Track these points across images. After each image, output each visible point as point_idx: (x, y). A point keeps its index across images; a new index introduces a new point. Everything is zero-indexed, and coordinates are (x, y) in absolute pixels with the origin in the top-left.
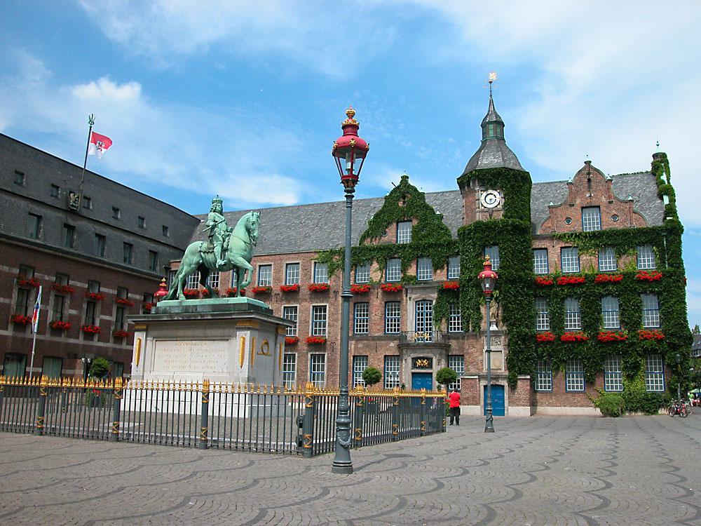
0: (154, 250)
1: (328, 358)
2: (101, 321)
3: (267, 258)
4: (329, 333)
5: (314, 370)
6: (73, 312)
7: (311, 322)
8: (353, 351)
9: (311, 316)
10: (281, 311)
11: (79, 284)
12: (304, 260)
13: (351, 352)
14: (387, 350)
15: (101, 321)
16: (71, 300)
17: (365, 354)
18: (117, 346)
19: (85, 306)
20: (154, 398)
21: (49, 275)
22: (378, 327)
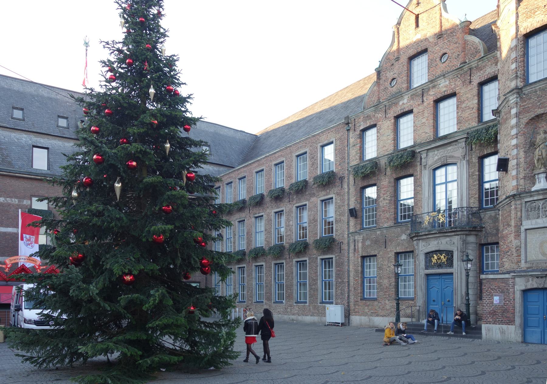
1: (336, 263)
3: (279, 154)
4: (337, 231)
5: (325, 278)
8: (360, 250)
10: (292, 212)
12: (311, 146)
13: (358, 252)
17: (373, 253)
22: (388, 215)
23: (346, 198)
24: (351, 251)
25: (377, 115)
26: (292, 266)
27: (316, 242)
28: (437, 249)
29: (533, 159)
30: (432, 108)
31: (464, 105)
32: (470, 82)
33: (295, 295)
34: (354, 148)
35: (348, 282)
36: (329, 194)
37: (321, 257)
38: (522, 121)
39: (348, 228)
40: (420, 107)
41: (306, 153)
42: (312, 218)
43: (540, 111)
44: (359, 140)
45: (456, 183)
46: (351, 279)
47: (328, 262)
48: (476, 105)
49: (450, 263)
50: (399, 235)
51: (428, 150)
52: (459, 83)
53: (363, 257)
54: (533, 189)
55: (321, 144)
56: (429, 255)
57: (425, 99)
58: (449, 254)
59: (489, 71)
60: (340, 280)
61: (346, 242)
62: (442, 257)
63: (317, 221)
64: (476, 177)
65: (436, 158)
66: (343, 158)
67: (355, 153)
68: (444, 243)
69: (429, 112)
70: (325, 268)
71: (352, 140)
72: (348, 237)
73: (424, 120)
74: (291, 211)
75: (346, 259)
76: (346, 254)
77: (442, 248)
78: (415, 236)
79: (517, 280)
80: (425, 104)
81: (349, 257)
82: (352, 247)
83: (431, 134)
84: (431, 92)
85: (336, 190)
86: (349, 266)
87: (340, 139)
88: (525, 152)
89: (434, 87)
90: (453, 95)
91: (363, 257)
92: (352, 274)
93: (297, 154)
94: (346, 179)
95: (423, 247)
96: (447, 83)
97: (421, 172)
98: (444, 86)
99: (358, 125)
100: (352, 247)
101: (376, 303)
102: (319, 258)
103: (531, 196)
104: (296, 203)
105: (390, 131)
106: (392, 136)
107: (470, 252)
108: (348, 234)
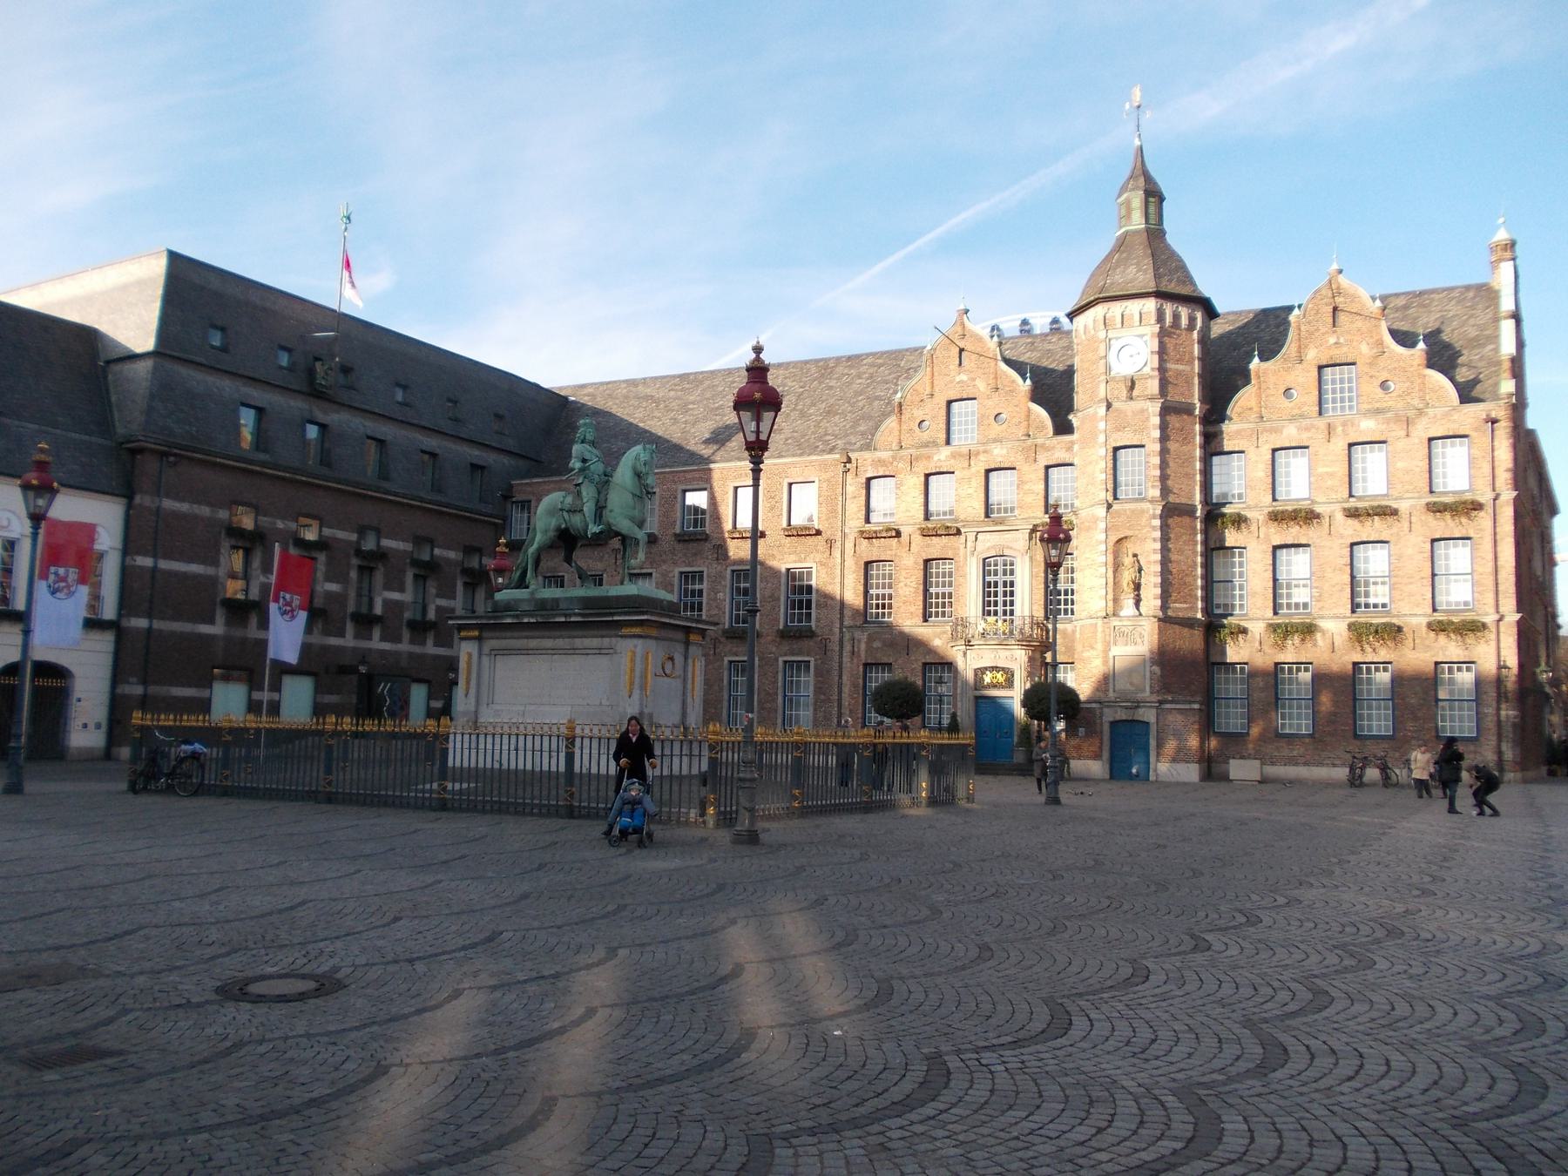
0: (481, 463)
2: (386, 603)
4: (818, 620)
6: (333, 587)
7: (783, 599)
8: (863, 654)
9: (783, 588)
10: (724, 578)
11: (341, 534)
15: (386, 603)
16: (329, 564)
17: (885, 660)
18: (417, 649)
19: (353, 574)
20: (497, 747)
21: (283, 518)
22: (913, 609)
26: (721, 667)
35: (840, 700)
36: (805, 560)
42: (767, 593)
61: (836, 638)
63: (778, 599)
74: (721, 576)
76: (836, 658)
81: (841, 664)
85: (818, 557)
86: (840, 677)
91: (866, 665)
92: (846, 690)
94: (838, 544)
100: (847, 648)
102: (781, 659)
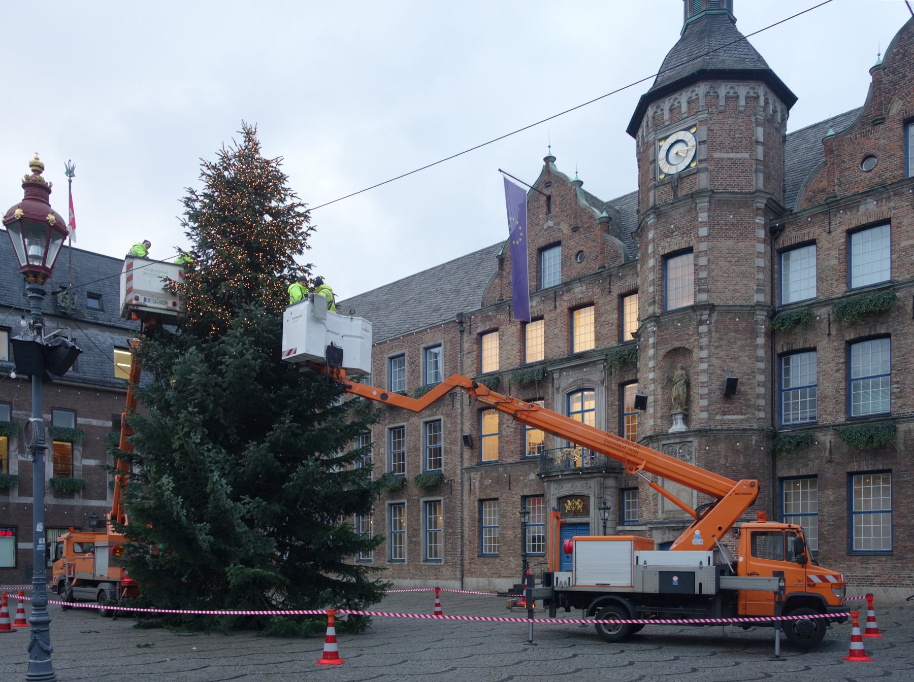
4: (446, 464)
5: (431, 527)
8: (477, 491)
10: (384, 435)
13: (475, 493)
14: (525, 486)
17: (494, 496)
22: (512, 447)
23: (459, 421)
24: (466, 492)
25: (498, 316)
27: (418, 479)
28: (571, 493)
29: (670, 397)
30: (566, 317)
31: (602, 319)
32: (610, 292)
33: (387, 551)
34: (469, 355)
37: (425, 499)
38: (659, 352)
39: (462, 461)
40: (552, 314)
41: (403, 355)
42: (411, 445)
43: (677, 344)
44: (475, 346)
45: (593, 413)
46: (466, 528)
47: (432, 506)
48: (616, 321)
49: (586, 511)
50: (526, 474)
51: (561, 369)
52: (597, 290)
53: (481, 501)
54: (671, 431)
55: (425, 345)
56: (562, 500)
57: (558, 304)
58: (584, 498)
59: (629, 282)
60: (450, 531)
62: (577, 503)
64: (616, 408)
65: (571, 380)
66: (455, 367)
67: (470, 363)
68: (577, 487)
69: (562, 321)
70: (431, 514)
71: (466, 345)
72: (462, 474)
73: (557, 331)
74: (381, 434)
75: (458, 503)
76: (459, 496)
77: (577, 491)
78: (547, 476)
79: (654, 532)
80: (558, 310)
81: (462, 500)
82: (467, 487)
83: (565, 349)
84: (565, 298)
87: (451, 341)
88: (663, 388)
89: (568, 291)
90: (591, 304)
91: (481, 501)
93: (391, 355)
95: (554, 491)
96: (584, 288)
97: (553, 395)
98: (579, 292)
99: (474, 326)
100: (467, 487)
101: (497, 560)
102: (422, 500)
103: (668, 439)
104: (389, 423)
105: (515, 339)
106: (517, 346)
107: (608, 497)
108: (462, 470)
